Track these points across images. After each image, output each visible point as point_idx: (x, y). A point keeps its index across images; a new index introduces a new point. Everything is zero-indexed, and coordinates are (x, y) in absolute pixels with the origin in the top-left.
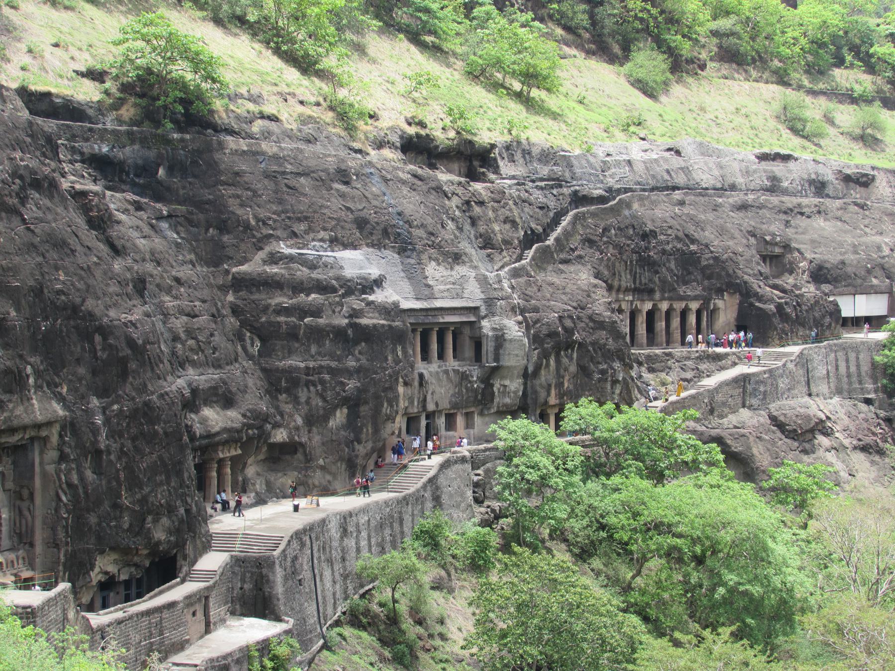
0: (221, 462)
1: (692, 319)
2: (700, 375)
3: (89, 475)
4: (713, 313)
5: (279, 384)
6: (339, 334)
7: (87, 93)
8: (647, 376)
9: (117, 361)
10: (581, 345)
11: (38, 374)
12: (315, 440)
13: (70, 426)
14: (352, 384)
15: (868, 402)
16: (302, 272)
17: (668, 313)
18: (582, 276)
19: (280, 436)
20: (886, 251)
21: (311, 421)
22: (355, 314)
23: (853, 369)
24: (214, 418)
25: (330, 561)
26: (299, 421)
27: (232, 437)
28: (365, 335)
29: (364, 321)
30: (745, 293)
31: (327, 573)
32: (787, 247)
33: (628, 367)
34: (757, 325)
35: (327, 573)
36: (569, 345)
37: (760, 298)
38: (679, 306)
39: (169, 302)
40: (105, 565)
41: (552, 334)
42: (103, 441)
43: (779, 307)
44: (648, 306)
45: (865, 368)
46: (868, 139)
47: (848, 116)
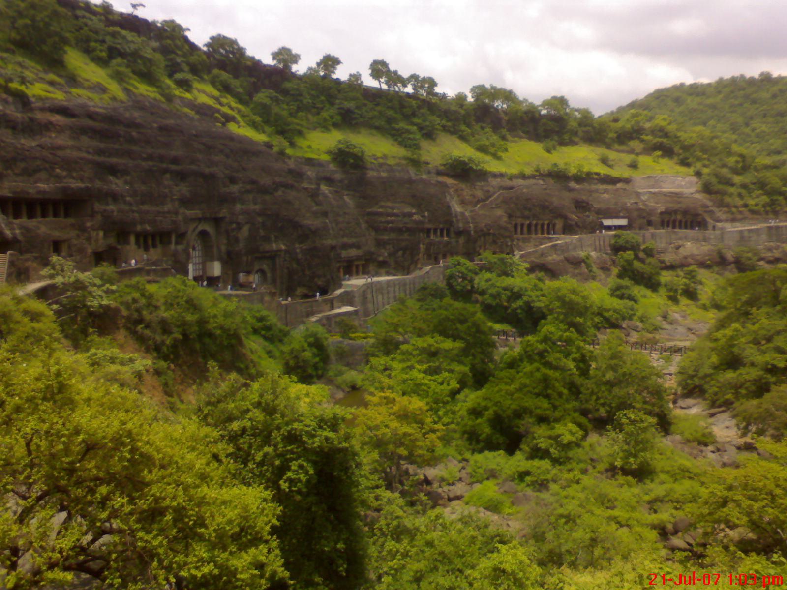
0: (357, 266)
1: (546, 227)
2: (541, 244)
3: (295, 266)
4: (554, 225)
5: (380, 244)
6: (400, 231)
7: (325, 158)
8: (521, 244)
9: (306, 234)
10: (494, 234)
11: (276, 237)
12: (392, 261)
13: (286, 251)
14: (404, 244)
15: (607, 254)
16: (389, 211)
17: (536, 225)
18: (499, 212)
19: (381, 258)
20: (629, 204)
21: (390, 255)
22: (405, 223)
23: (602, 243)
24: (353, 252)
25: (382, 294)
26: (386, 254)
27: (359, 258)
28: (409, 230)
29: (408, 226)
30: (565, 218)
31: (380, 297)
32: (588, 203)
33: (512, 241)
34: (568, 229)
35: (380, 297)
36: (489, 234)
37: (570, 220)
38: (540, 222)
39: (341, 219)
40: (300, 291)
41: (482, 230)
42: (300, 256)
43: (576, 223)
44: (528, 222)
45: (607, 243)
46: (634, 166)
47: (628, 158)
